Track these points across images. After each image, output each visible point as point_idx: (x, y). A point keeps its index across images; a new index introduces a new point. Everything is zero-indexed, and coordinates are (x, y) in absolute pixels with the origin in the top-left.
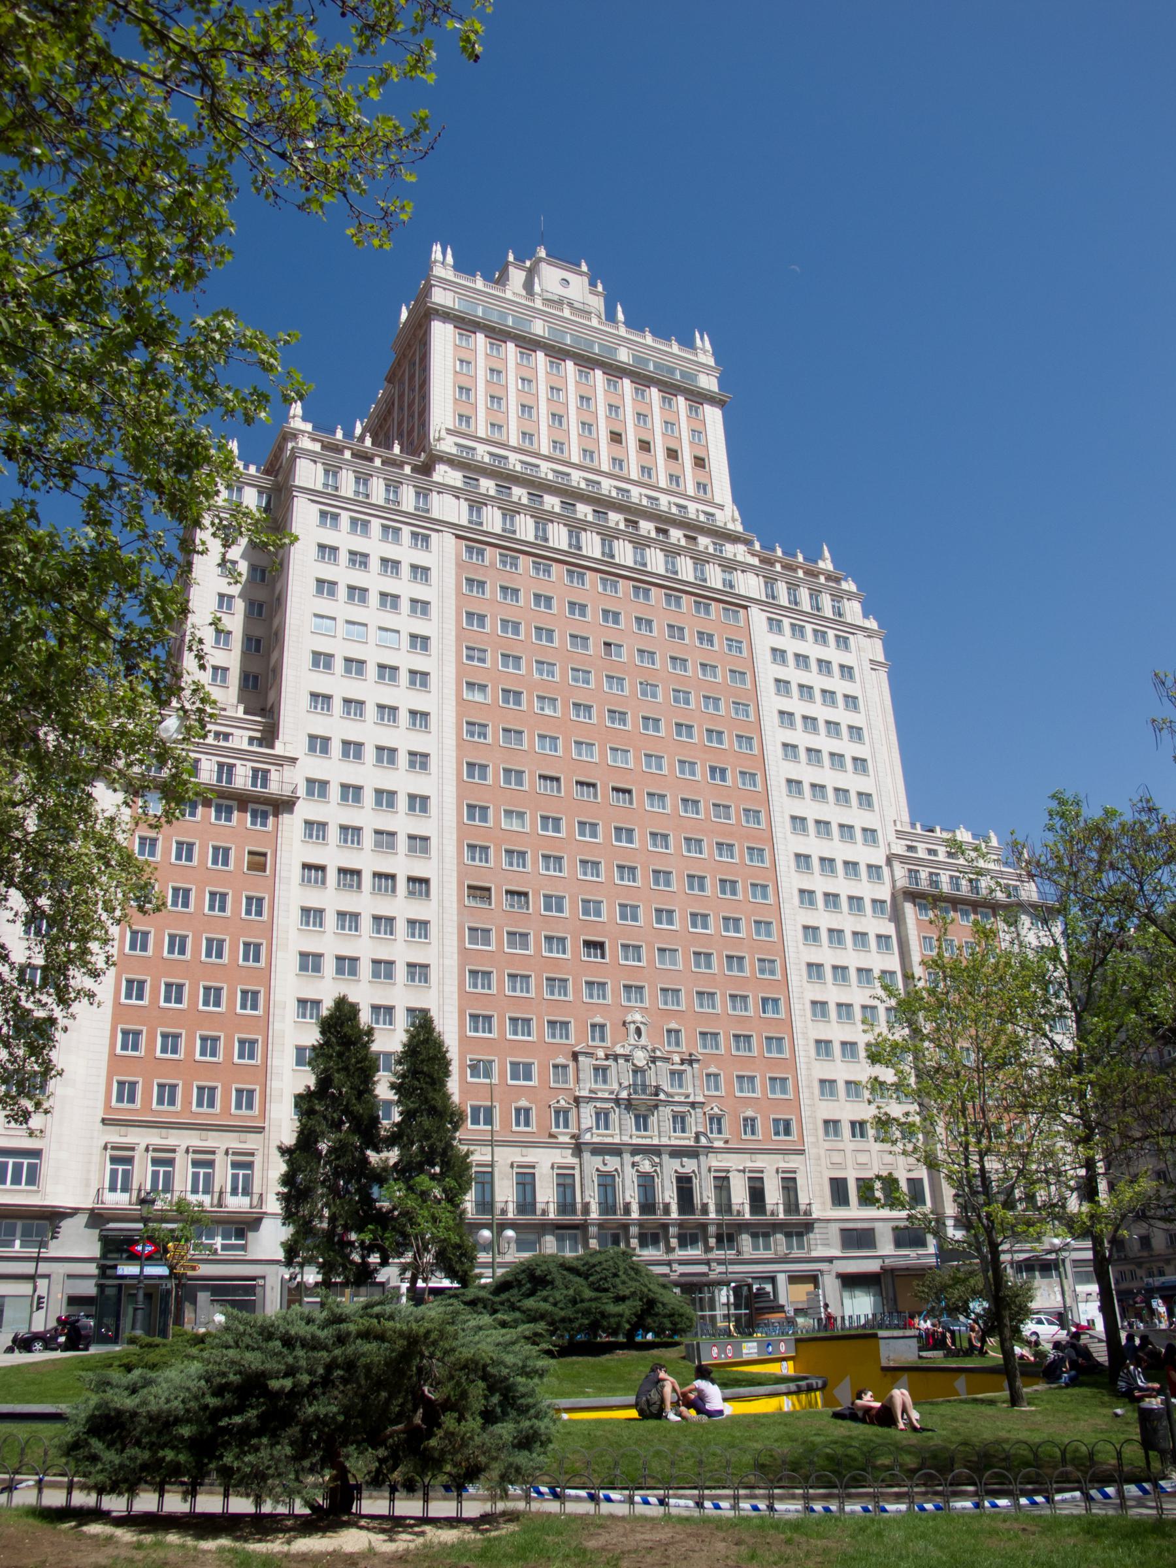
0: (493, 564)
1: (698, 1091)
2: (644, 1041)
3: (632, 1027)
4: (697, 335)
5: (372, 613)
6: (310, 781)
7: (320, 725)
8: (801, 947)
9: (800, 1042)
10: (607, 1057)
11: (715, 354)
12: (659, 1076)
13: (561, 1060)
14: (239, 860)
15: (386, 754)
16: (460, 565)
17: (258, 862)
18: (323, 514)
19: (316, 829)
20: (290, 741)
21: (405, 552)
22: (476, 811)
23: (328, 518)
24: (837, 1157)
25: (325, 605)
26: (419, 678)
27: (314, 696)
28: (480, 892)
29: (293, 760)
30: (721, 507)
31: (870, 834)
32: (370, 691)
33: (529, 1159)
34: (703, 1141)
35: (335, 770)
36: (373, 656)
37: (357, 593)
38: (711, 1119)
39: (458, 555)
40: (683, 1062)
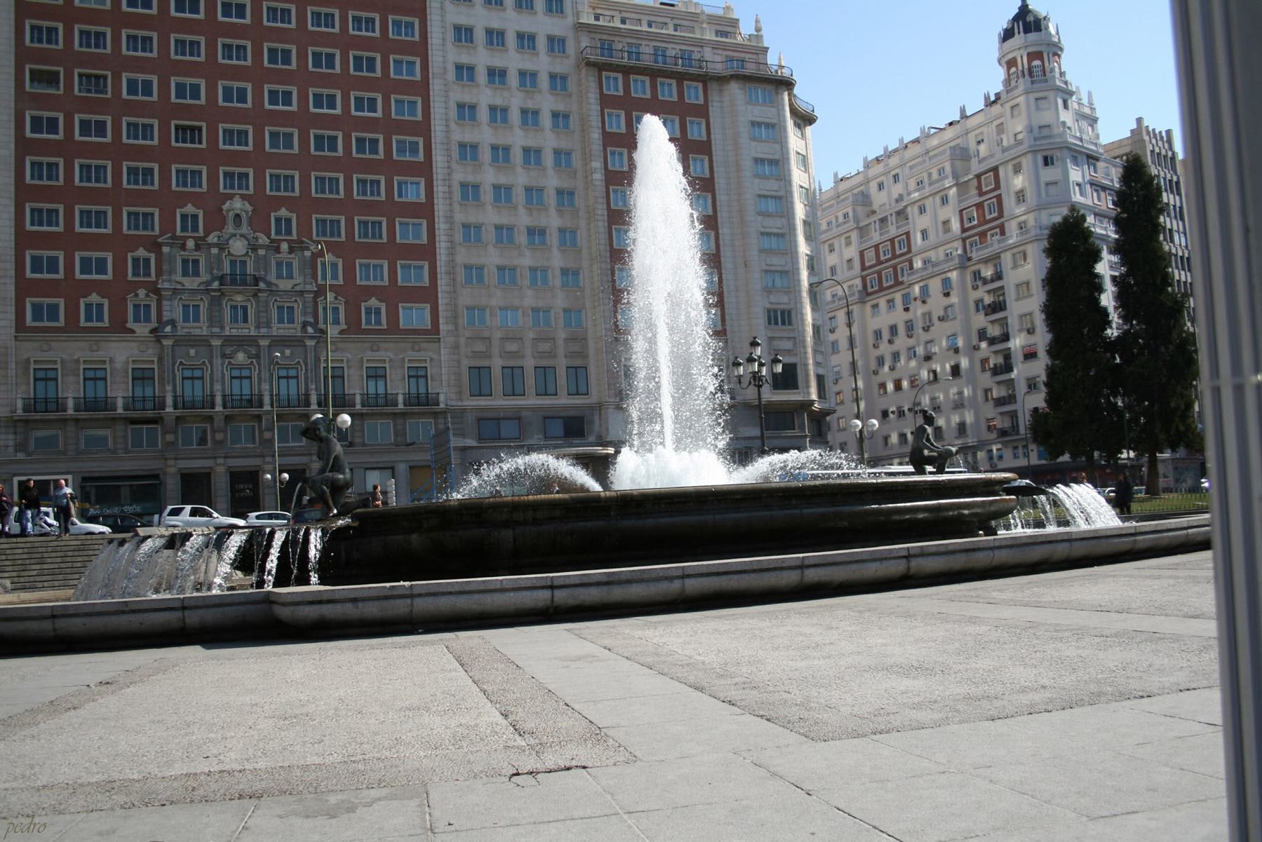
1: (309, 279)
3: (231, 214)
8: (453, 126)
9: (441, 226)
10: (198, 247)
24: (480, 347)
33: (101, 354)
34: (310, 330)
40: (291, 250)
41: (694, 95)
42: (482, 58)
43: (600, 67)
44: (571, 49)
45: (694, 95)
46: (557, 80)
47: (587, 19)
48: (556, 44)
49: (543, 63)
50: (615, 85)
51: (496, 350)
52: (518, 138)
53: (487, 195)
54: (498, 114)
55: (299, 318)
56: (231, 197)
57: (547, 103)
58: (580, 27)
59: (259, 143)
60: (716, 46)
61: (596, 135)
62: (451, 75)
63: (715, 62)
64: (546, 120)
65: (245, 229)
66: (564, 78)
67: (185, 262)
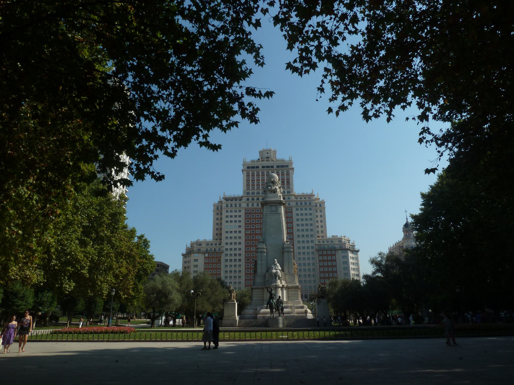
0: (250, 211)
5: (233, 224)
6: (226, 249)
7: (227, 241)
14: (217, 260)
15: (235, 243)
16: (246, 213)
17: (219, 260)
18: (226, 211)
19: (226, 255)
20: (223, 244)
21: (238, 214)
23: (227, 211)
25: (227, 224)
26: (240, 232)
27: (226, 237)
29: (223, 247)
31: (312, 241)
32: (233, 235)
35: (229, 247)
36: (233, 230)
37: (231, 222)
39: (245, 212)
41: (333, 252)
42: (302, 251)
43: (318, 251)
44: (315, 248)
45: (333, 252)
46: (313, 253)
47: (317, 243)
48: (312, 247)
49: (310, 250)
50: (321, 253)
52: (307, 262)
53: (303, 270)
54: (304, 259)
57: (311, 256)
58: (316, 245)
60: (337, 244)
61: (318, 261)
62: (297, 254)
63: (337, 247)
64: (311, 259)
66: (314, 252)
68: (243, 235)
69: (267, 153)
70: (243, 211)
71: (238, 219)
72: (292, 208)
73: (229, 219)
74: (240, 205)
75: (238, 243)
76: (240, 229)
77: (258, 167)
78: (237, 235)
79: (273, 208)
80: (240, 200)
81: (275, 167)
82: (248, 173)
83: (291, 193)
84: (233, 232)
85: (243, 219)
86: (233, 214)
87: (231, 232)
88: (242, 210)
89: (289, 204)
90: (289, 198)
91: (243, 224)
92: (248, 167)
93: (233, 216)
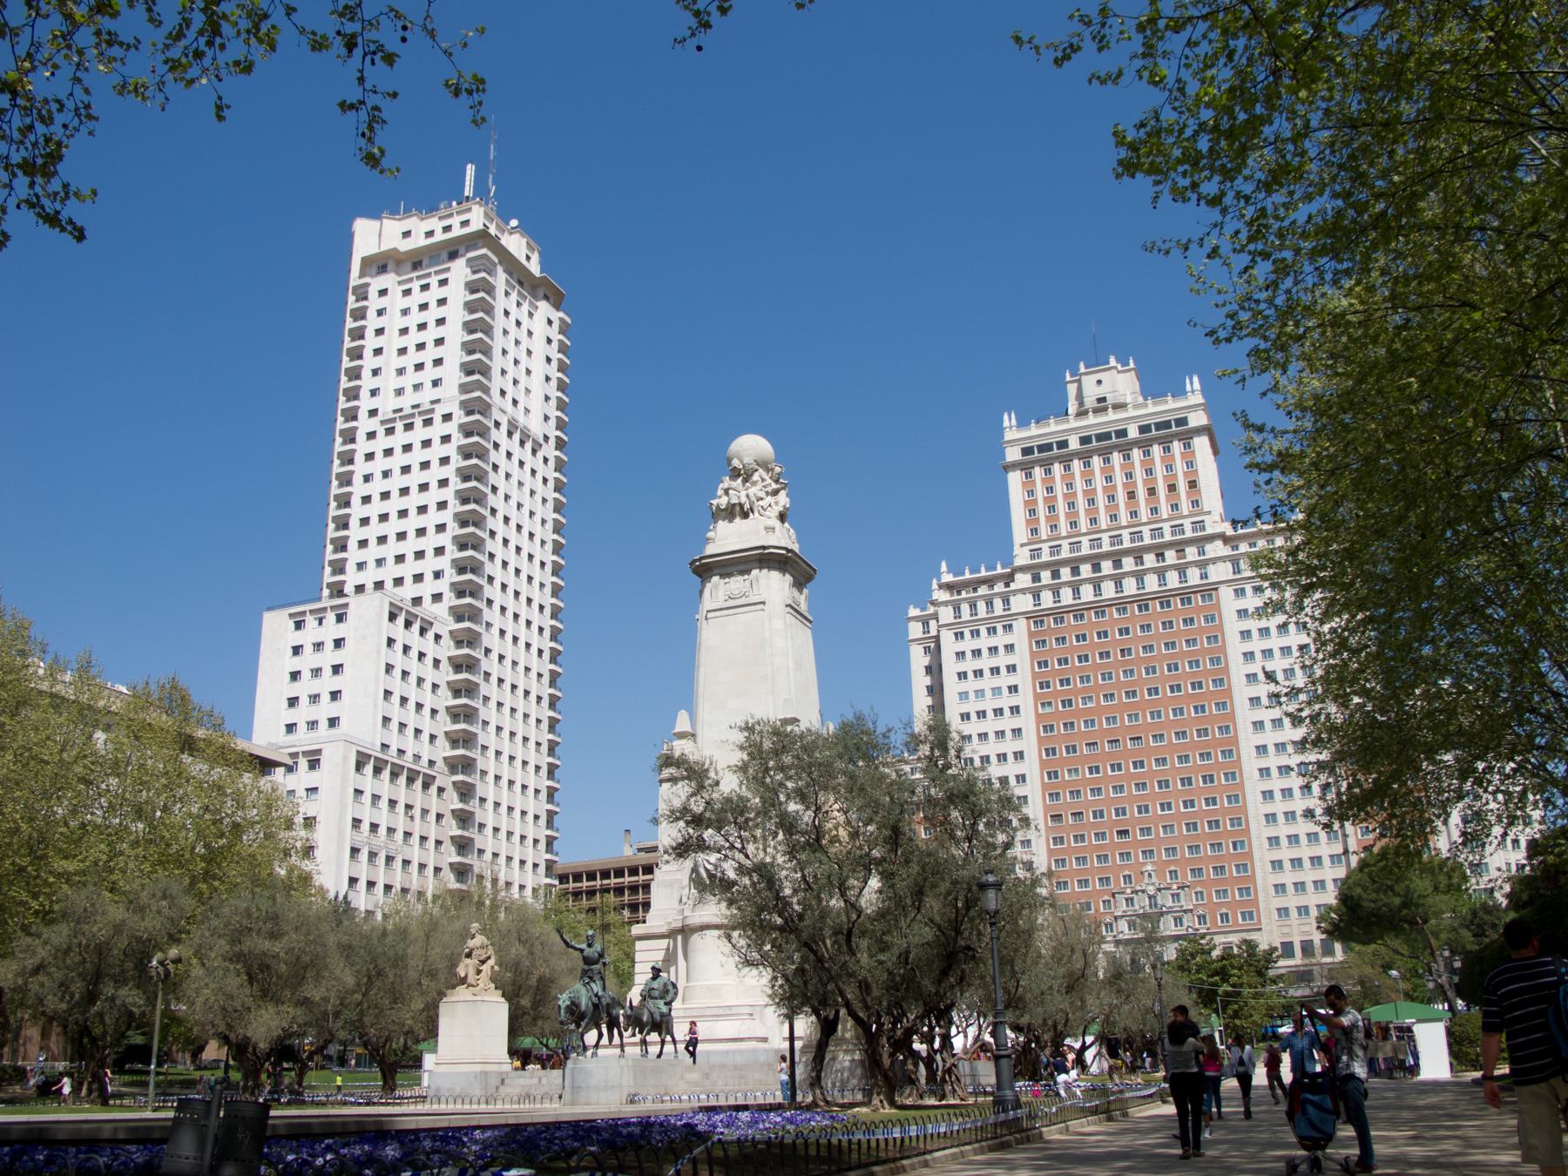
0: (1049, 626)
2: (1154, 879)
4: (1188, 381)
5: (987, 682)
9: (1257, 864)
11: (1204, 392)
12: (1166, 900)
13: (1106, 898)
16: (1031, 634)
18: (956, 634)
21: (1000, 640)
22: (1053, 775)
23: (959, 636)
24: (1285, 930)
28: (1057, 818)
30: (1209, 513)
37: (978, 673)
38: (1199, 917)
39: (1029, 628)
51: (1296, 930)
55: (1186, 924)
56: (1144, 864)
59: (1157, 834)
65: (1154, 879)
67: (1127, 900)
68: (1027, 721)
69: (1099, 382)
70: (1021, 626)
71: (1002, 660)
72: (1216, 589)
73: (969, 665)
74: (1006, 601)
75: (1010, 757)
76: (1014, 701)
77: (1063, 444)
78: (1007, 723)
79: (737, 583)
80: (1007, 585)
81: (1133, 433)
82: (1028, 475)
83: (1209, 531)
84: (990, 714)
85: (1022, 658)
86: (984, 642)
87: (982, 714)
88: (1014, 623)
89: (1204, 576)
90: (1202, 552)
91: (1024, 678)
92: (1027, 451)
93: (985, 652)
